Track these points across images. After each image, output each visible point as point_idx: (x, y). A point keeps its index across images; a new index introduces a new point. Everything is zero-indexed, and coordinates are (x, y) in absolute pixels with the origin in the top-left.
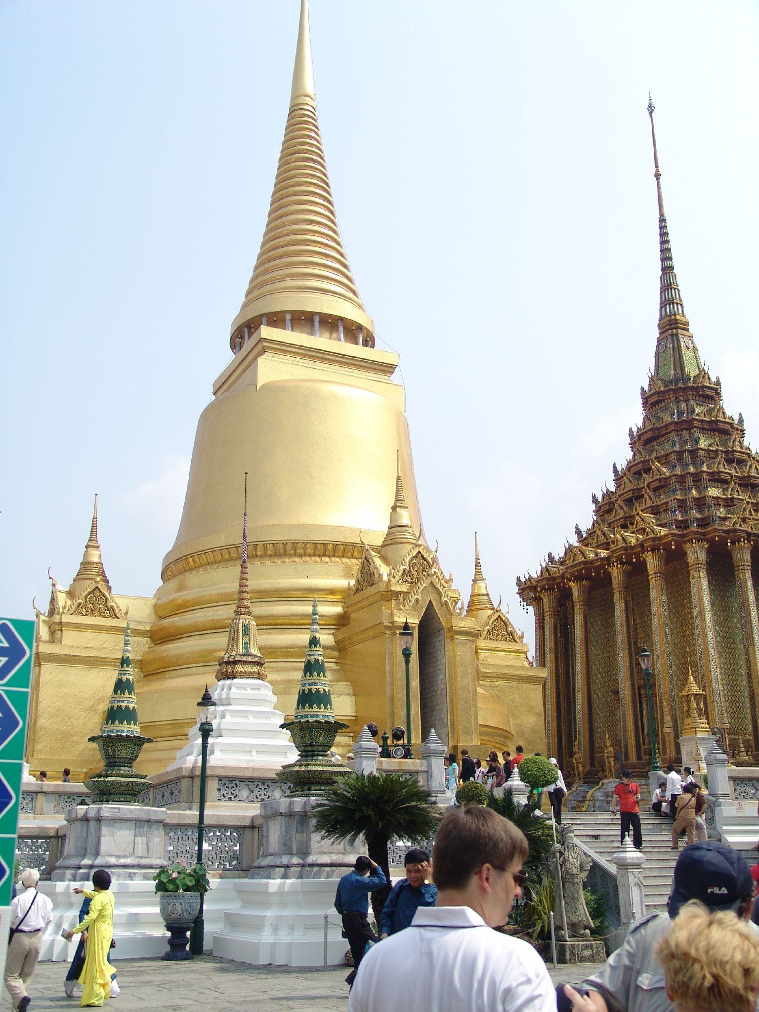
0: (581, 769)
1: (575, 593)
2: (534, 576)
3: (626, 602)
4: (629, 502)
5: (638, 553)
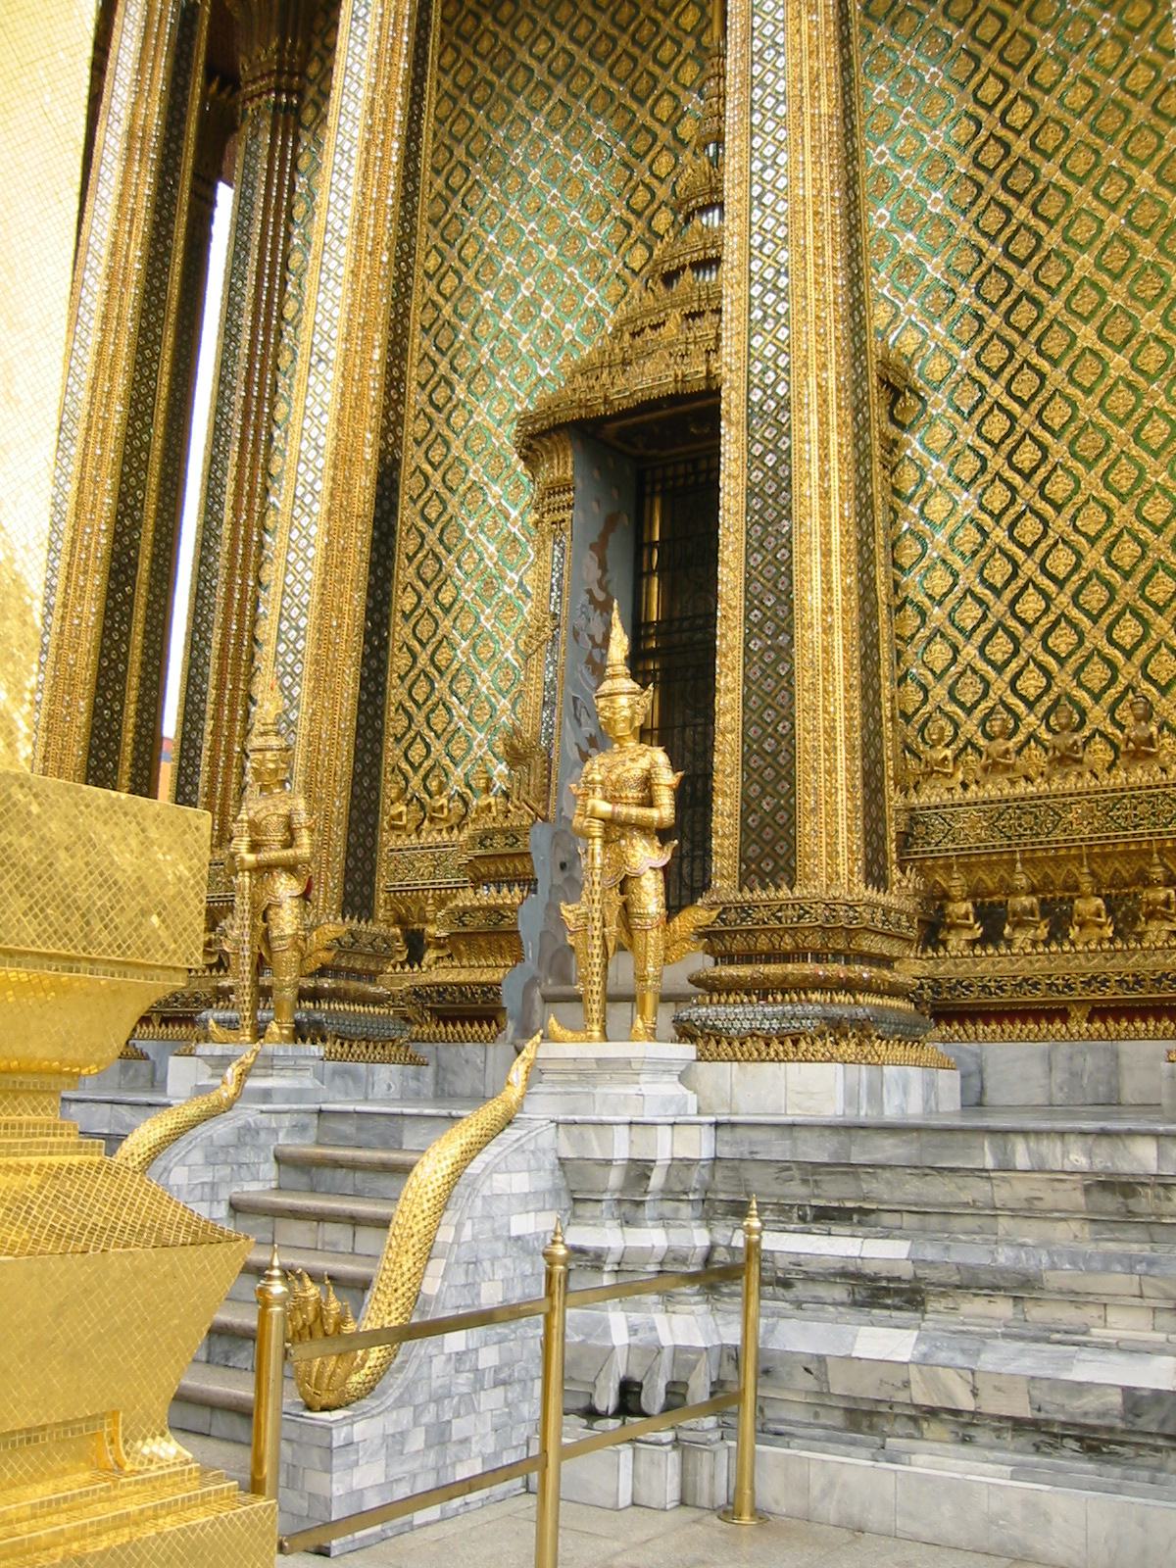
0: (287, 920)
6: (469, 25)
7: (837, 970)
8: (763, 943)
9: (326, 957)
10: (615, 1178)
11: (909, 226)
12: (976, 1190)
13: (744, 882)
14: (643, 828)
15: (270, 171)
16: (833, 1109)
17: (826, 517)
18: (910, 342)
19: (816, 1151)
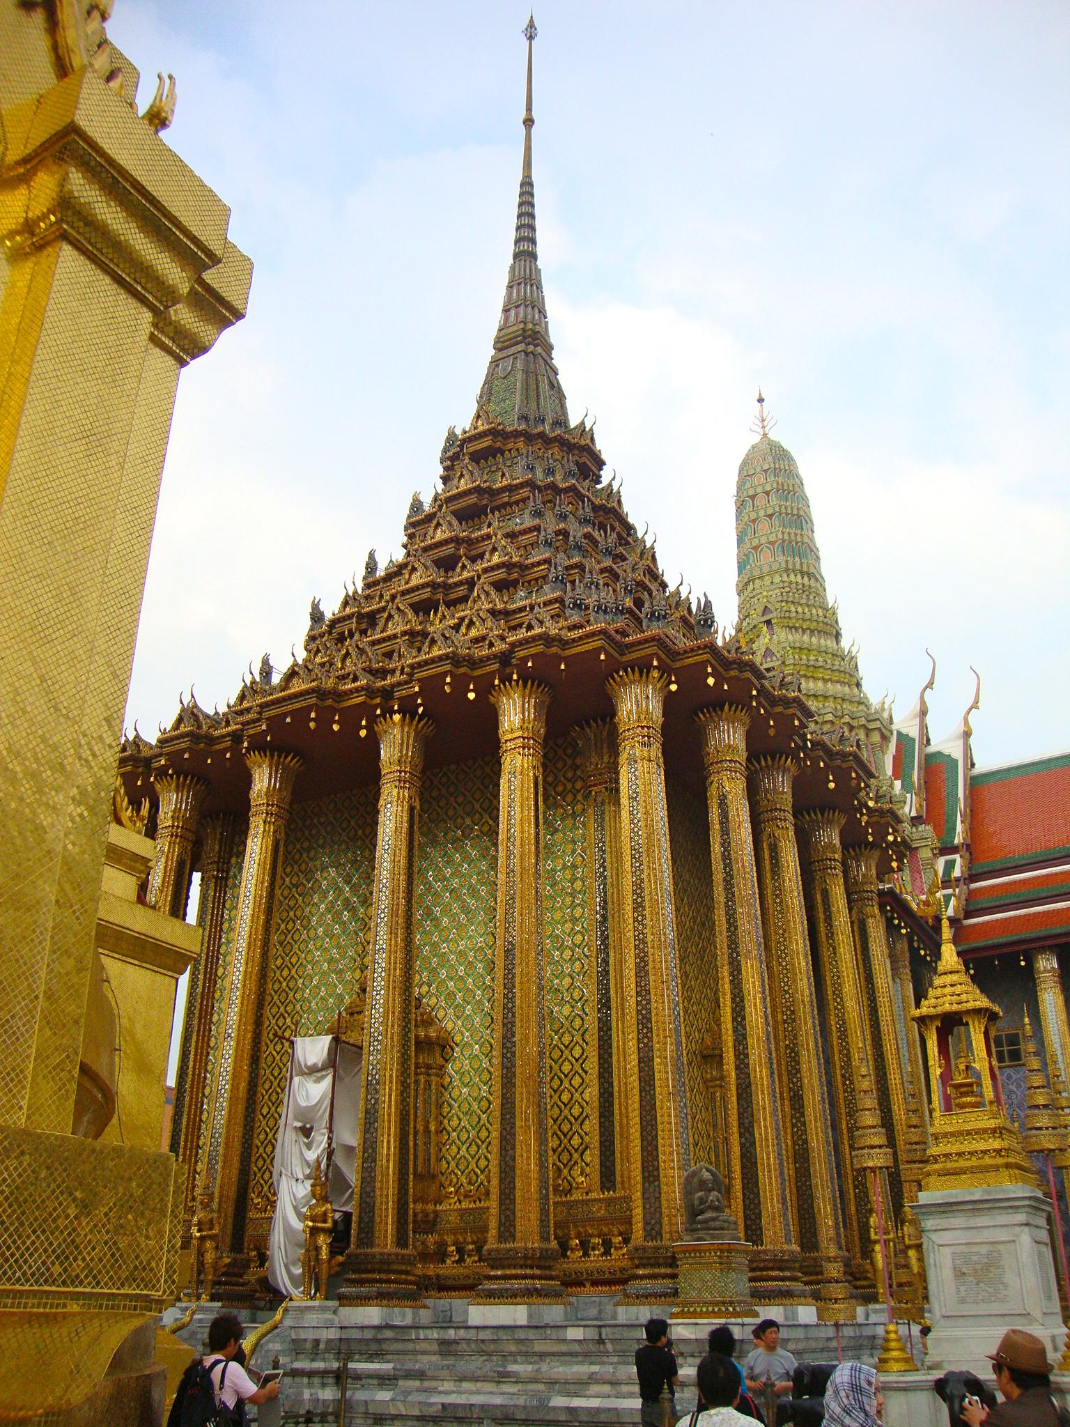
0: (209, 1257)
1: (262, 780)
2: (151, 737)
3: (412, 809)
4: (423, 608)
5: (491, 675)
6: (297, 856)
7: (383, 1276)
8: (363, 1267)
9: (224, 1270)
10: (308, 1346)
11: (451, 979)
12: (410, 1346)
13: (358, 1246)
14: (323, 1230)
15: (213, 908)
16: (376, 1321)
17: (389, 1122)
18: (450, 1026)
19: (368, 1334)
